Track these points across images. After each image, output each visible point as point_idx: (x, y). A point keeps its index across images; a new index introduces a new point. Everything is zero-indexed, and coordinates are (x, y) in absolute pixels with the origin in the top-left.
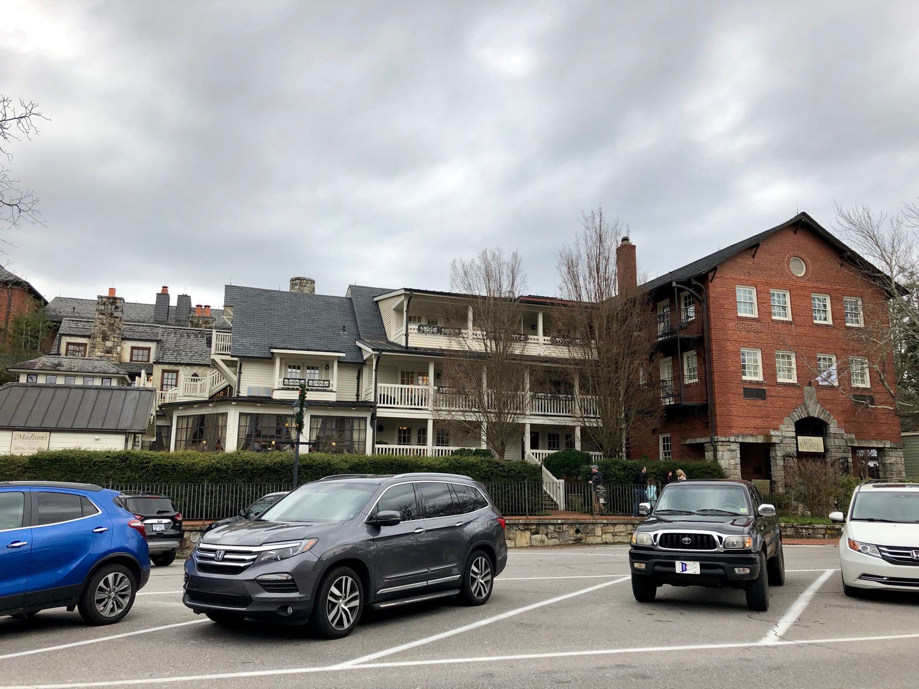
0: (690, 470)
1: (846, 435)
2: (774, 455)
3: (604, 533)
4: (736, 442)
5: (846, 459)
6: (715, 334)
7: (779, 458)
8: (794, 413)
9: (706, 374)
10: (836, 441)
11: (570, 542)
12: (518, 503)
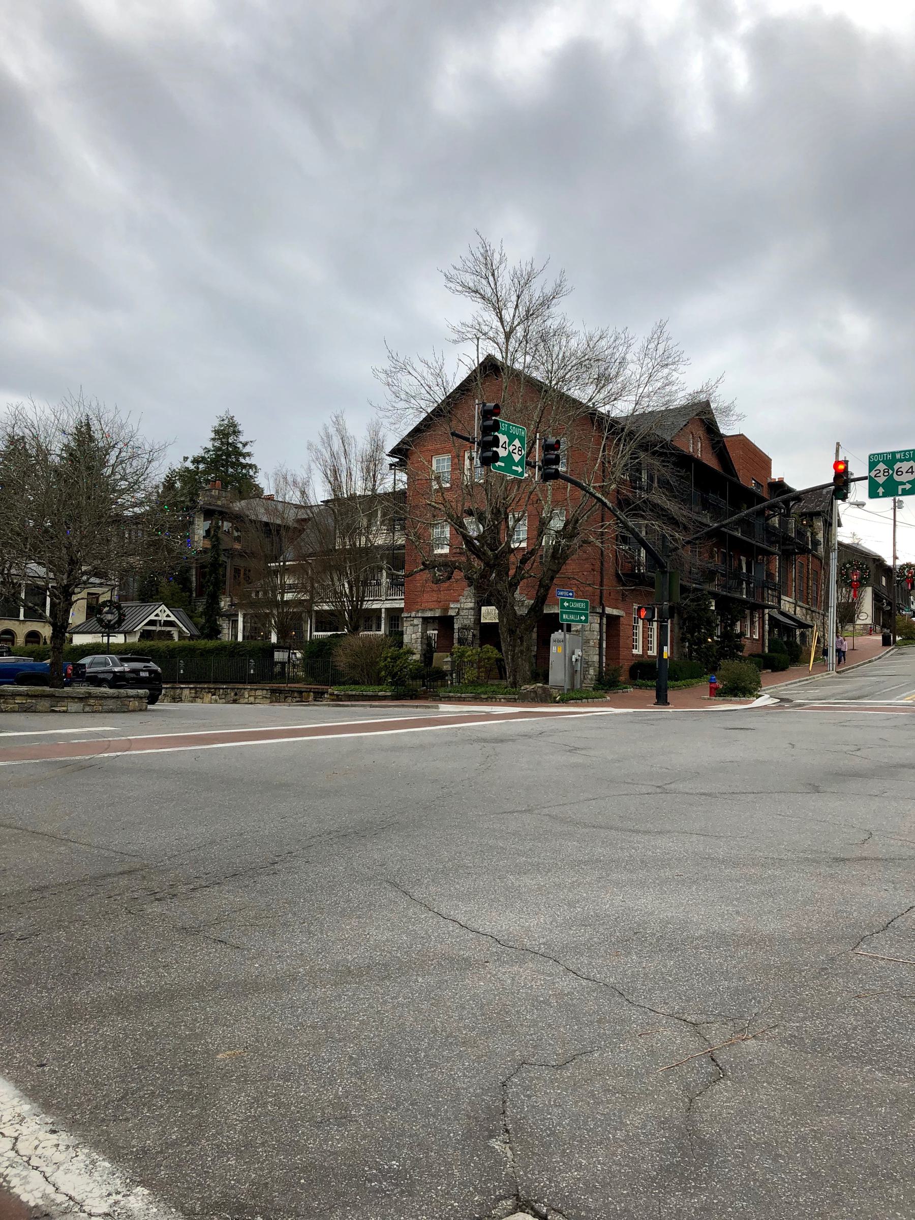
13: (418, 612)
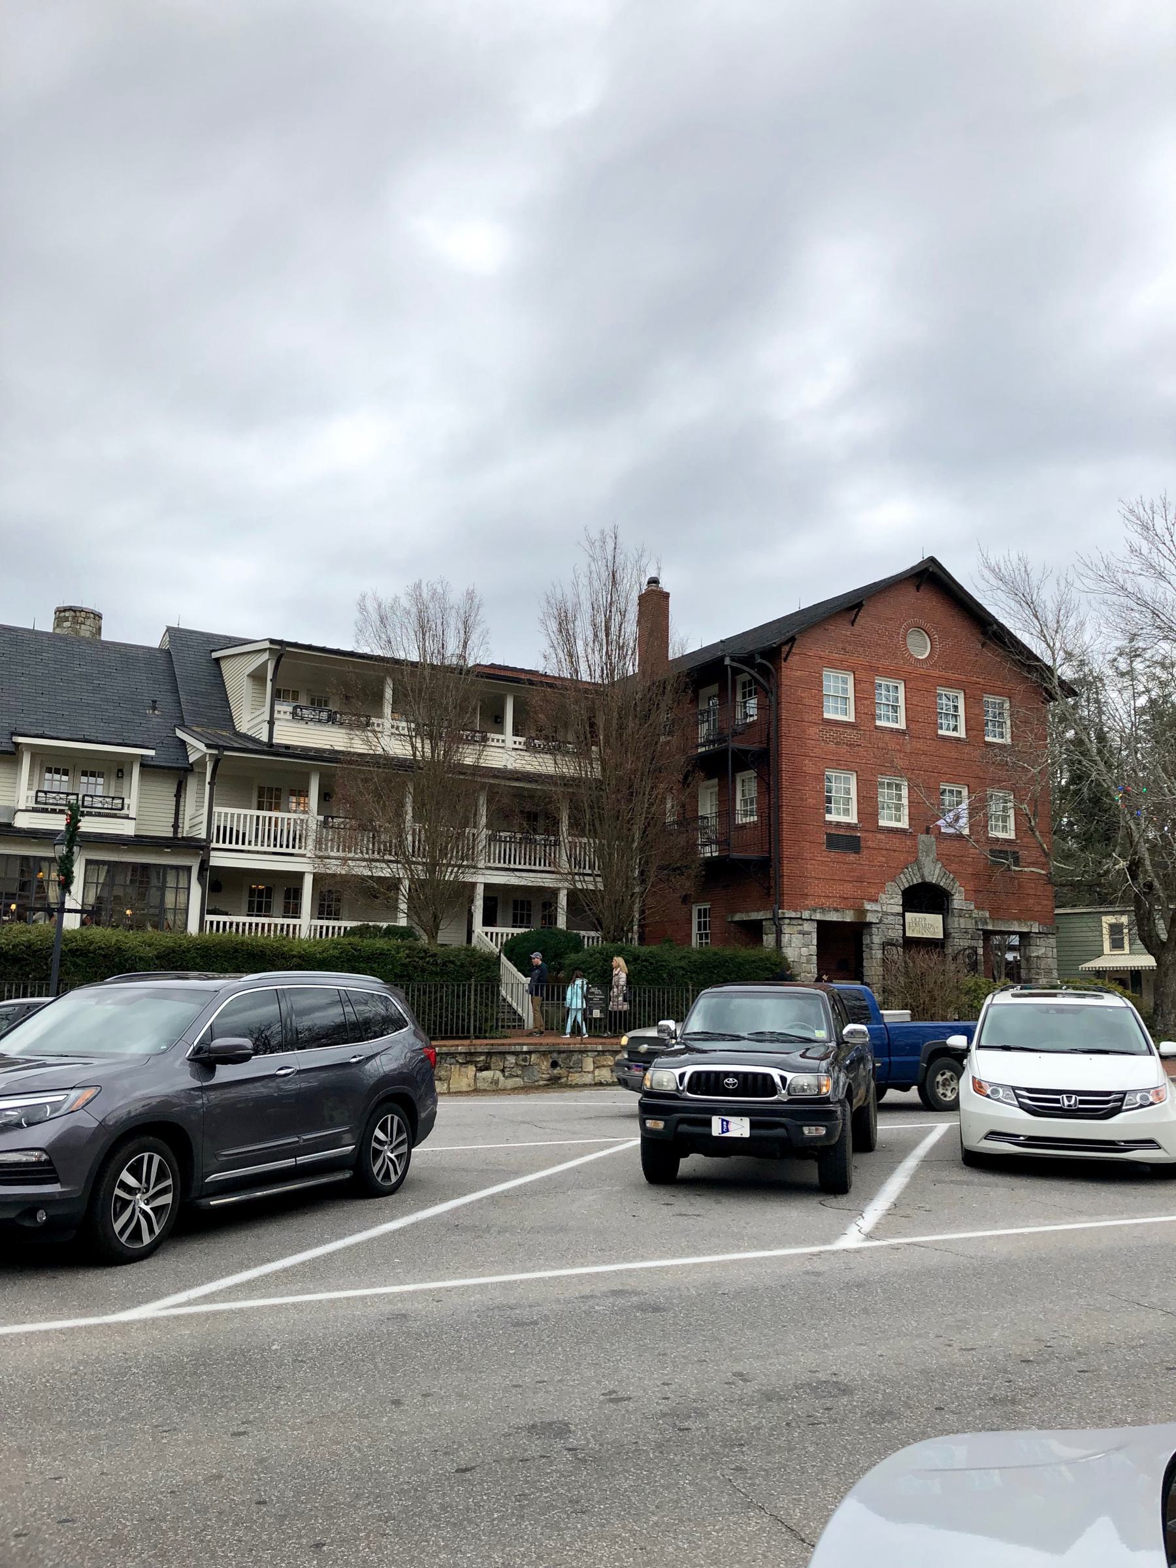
0: (740, 963)
1: (976, 911)
2: (869, 941)
3: (598, 1067)
4: (811, 920)
5: (975, 949)
6: (787, 746)
7: (875, 946)
8: (902, 876)
9: (769, 808)
10: (962, 920)
11: (541, 1083)
12: (458, 1017)
13: (815, 911)
